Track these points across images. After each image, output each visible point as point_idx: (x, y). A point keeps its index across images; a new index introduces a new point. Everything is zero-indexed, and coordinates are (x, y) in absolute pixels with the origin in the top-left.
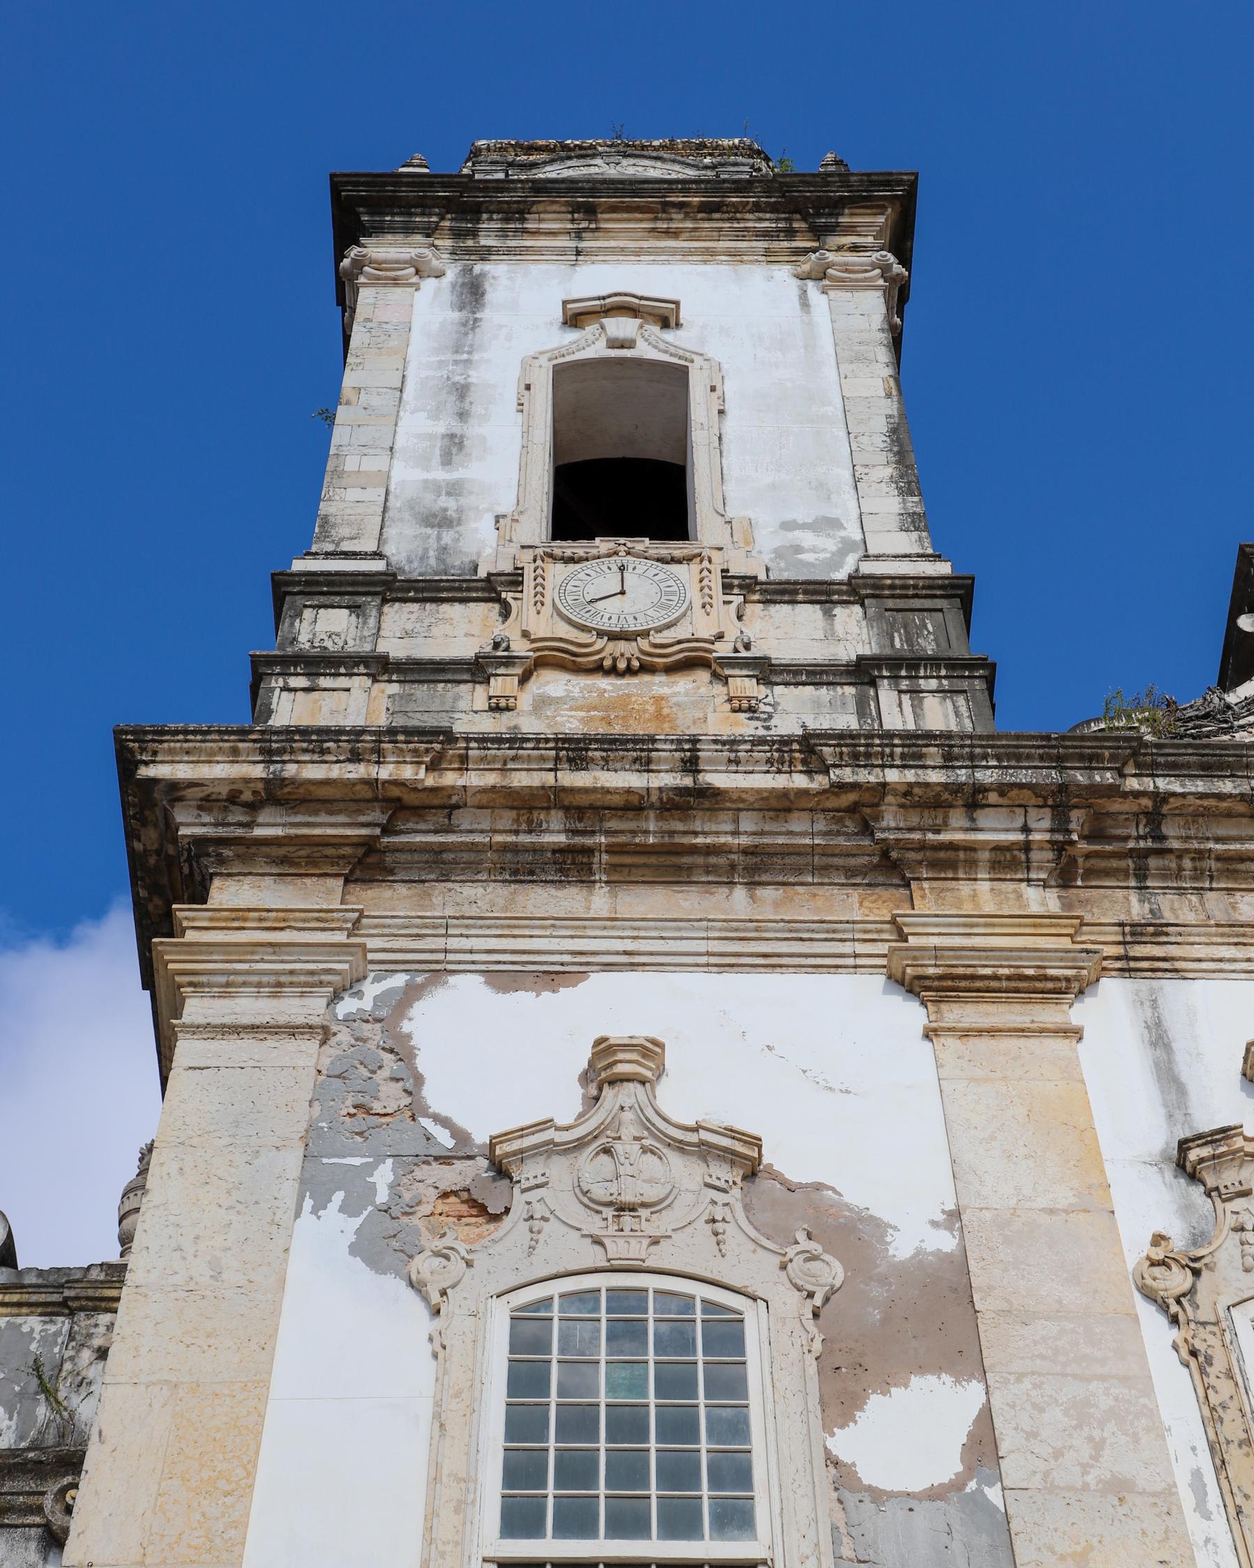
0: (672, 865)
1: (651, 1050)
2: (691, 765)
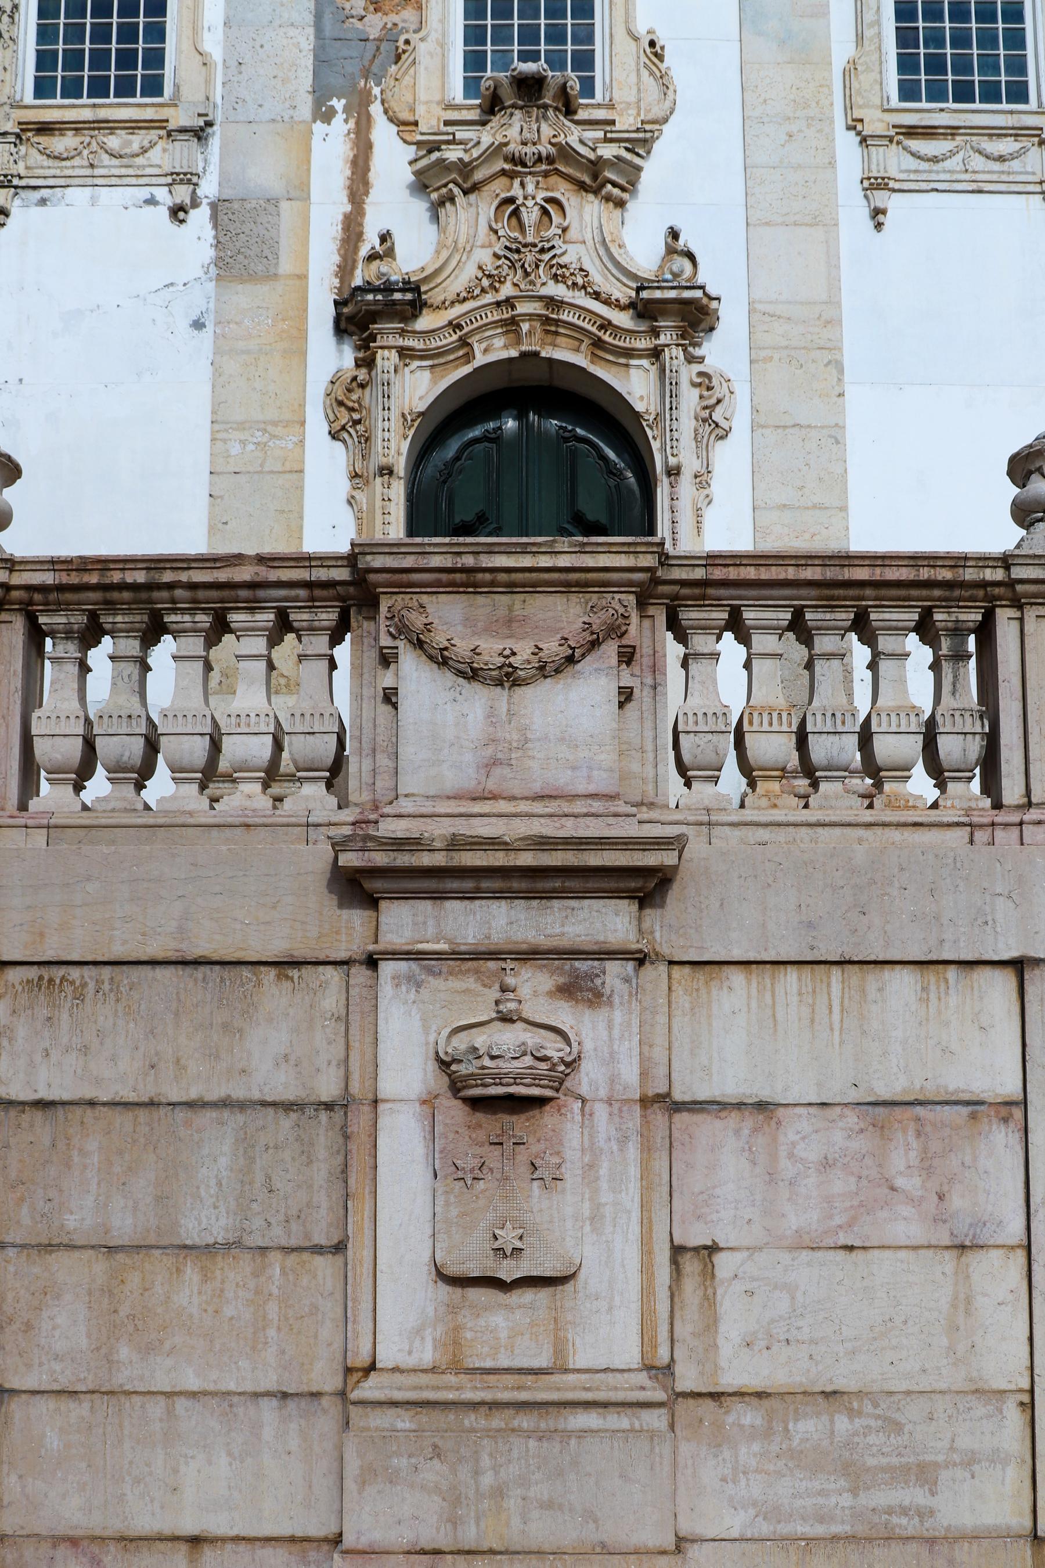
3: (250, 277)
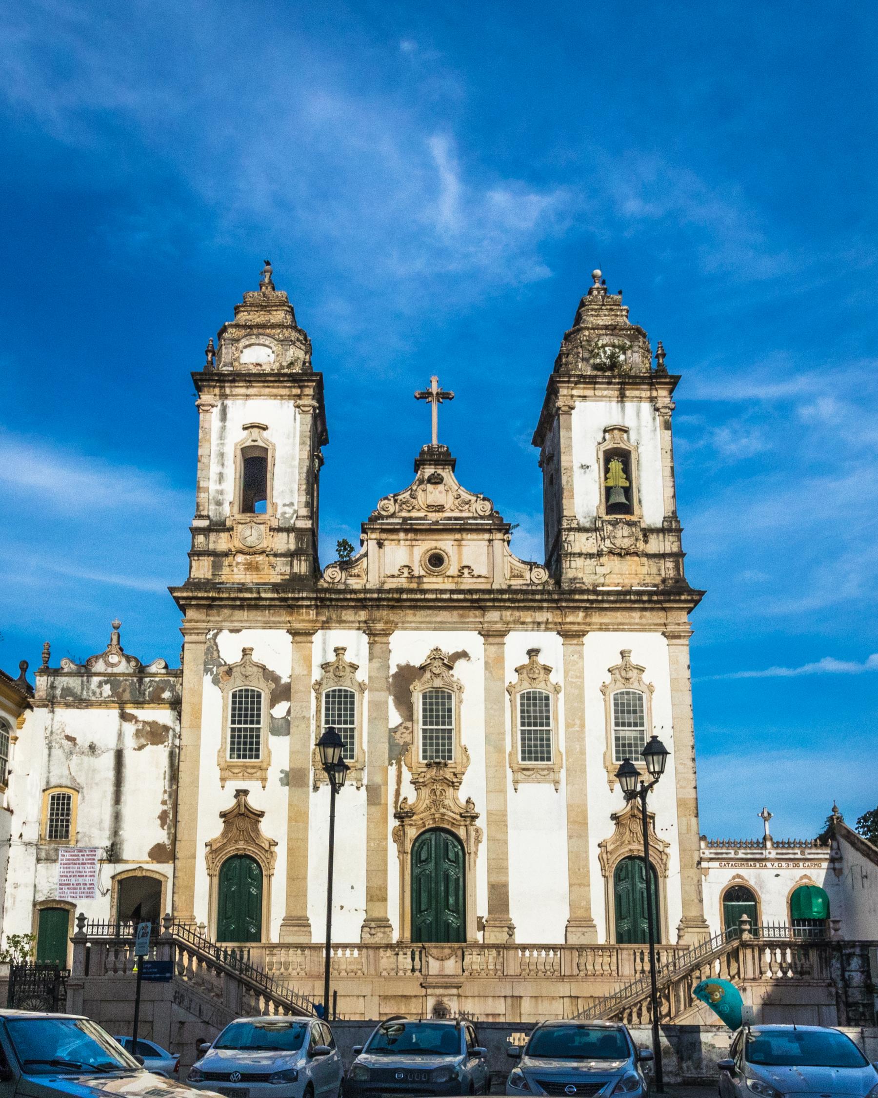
0: (256, 607)
1: (252, 649)
2: (259, 593)
3: (374, 804)
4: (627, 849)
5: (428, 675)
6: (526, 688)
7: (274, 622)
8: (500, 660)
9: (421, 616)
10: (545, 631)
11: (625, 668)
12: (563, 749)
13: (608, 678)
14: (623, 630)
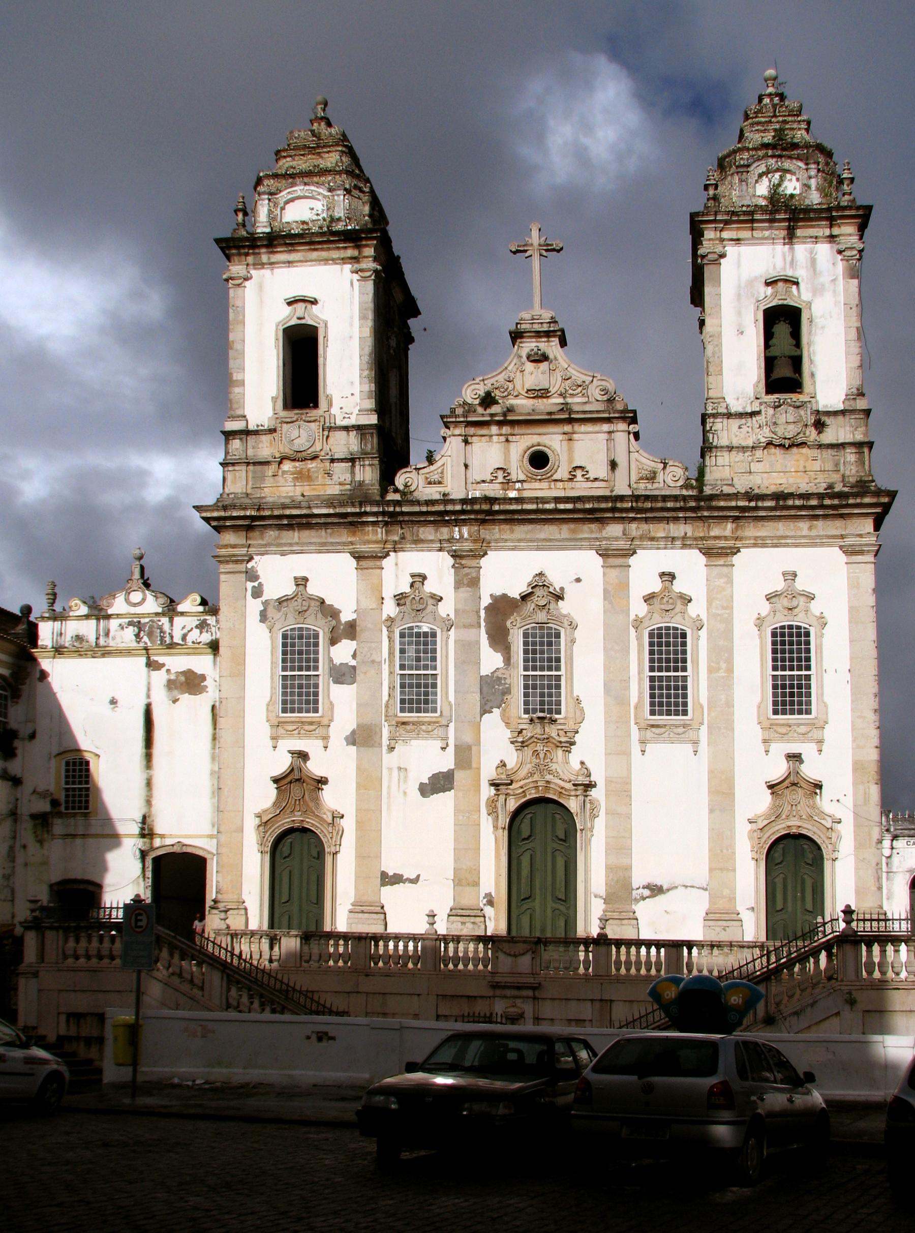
4: (783, 826)
5: (530, 606)
6: (658, 622)
7: (332, 544)
8: (624, 586)
9: (521, 531)
10: (682, 548)
11: (789, 594)
12: (704, 700)
13: (765, 608)
14: (786, 545)
